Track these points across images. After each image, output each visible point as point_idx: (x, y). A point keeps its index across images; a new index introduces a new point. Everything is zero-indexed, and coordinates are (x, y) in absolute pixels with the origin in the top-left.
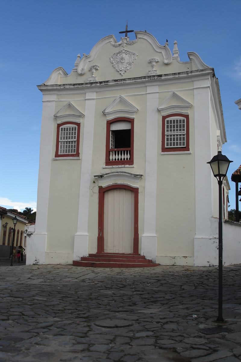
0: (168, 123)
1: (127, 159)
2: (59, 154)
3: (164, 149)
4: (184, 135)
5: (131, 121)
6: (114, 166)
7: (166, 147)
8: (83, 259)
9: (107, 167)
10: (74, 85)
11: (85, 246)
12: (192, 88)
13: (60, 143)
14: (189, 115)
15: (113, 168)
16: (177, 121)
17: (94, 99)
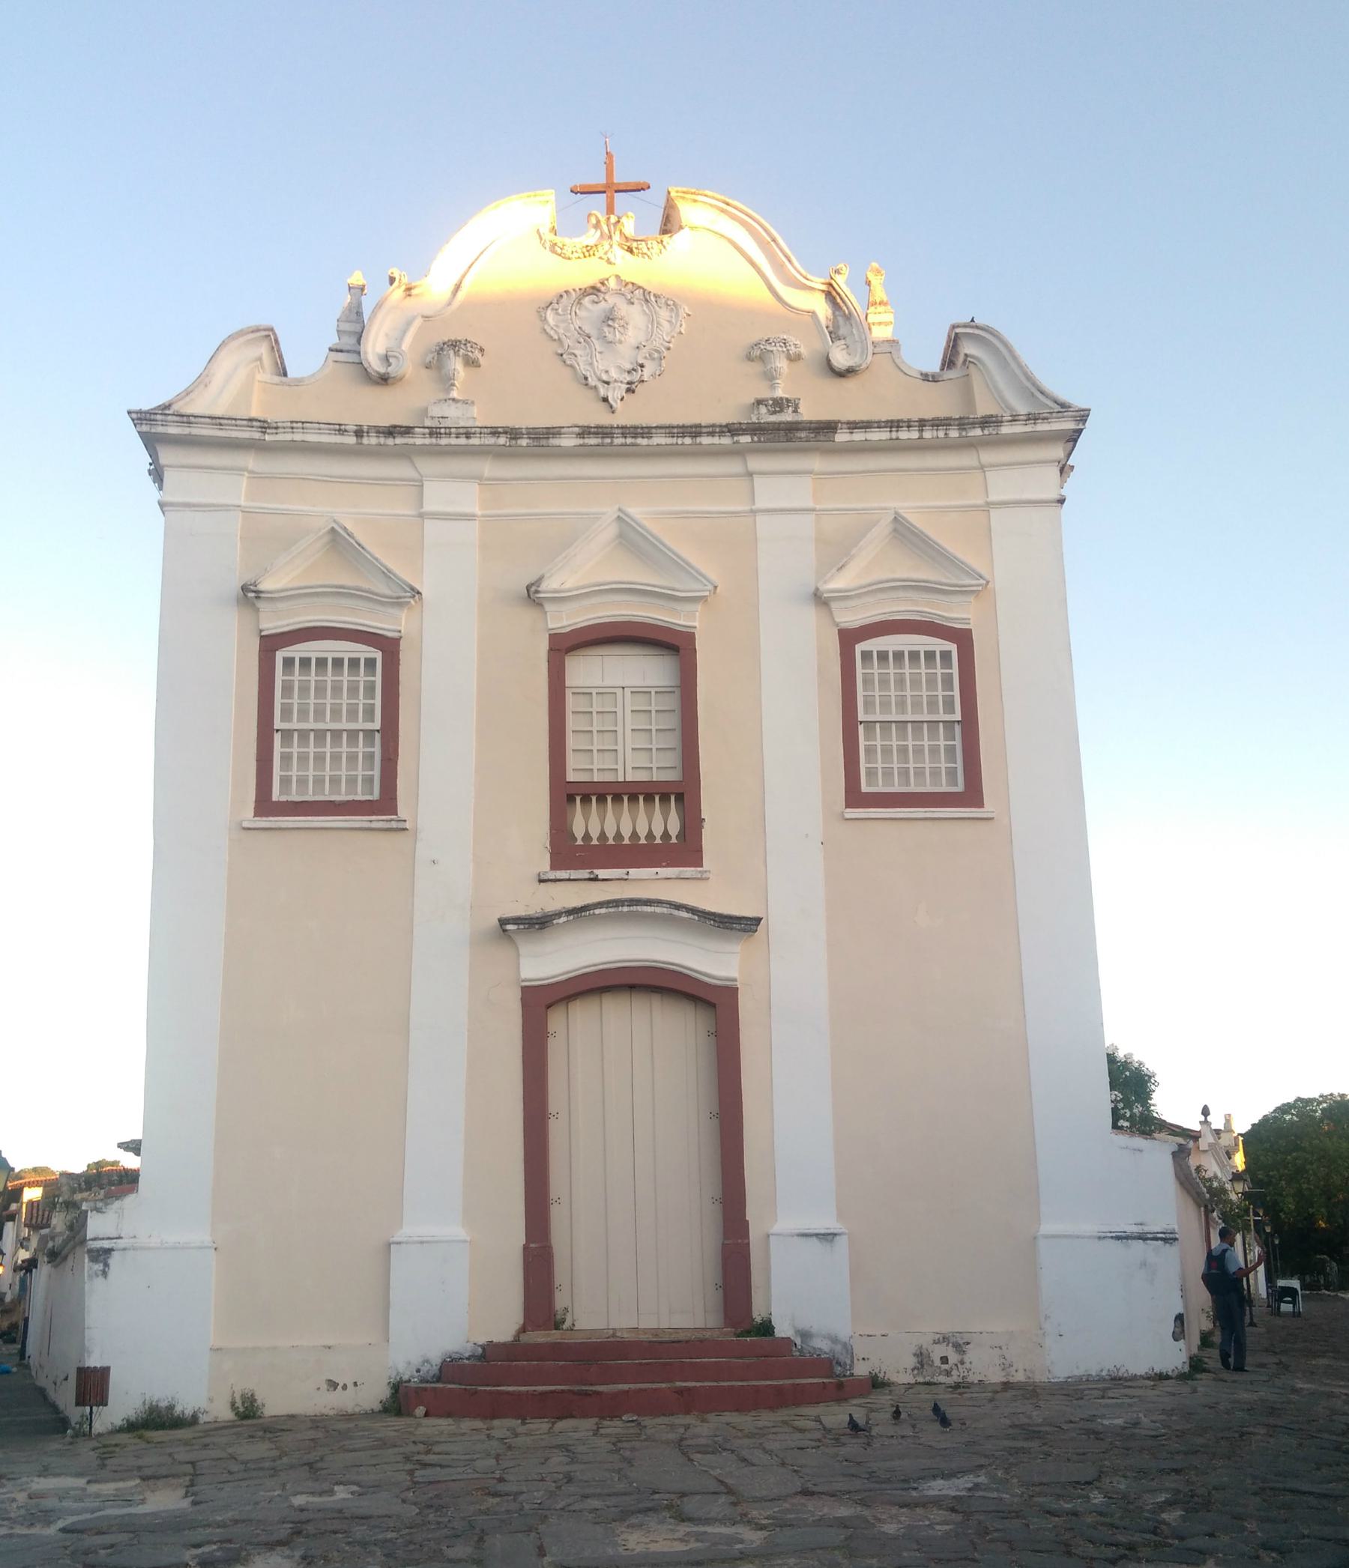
1: (666, 835)
2: (276, 796)
6: (602, 873)
8: (451, 1368)
11: (451, 1300)
12: (980, 502)
13: (277, 738)
14: (970, 630)
15: (596, 879)
17: (469, 517)
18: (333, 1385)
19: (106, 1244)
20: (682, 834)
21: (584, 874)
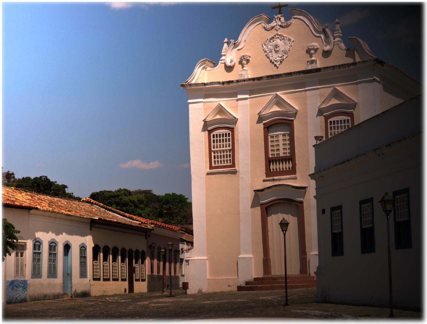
0: (331, 124)
2: (213, 165)
6: (275, 178)
8: (247, 283)
10: (223, 83)
13: (213, 153)
16: (341, 121)
18: (229, 286)
19: (188, 259)
20: (292, 168)
21: (272, 178)
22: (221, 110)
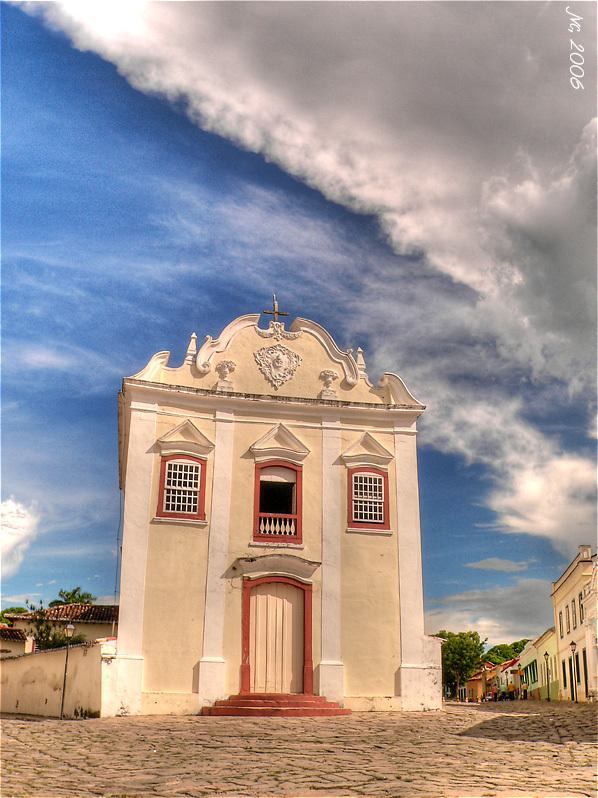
3: (351, 523)
4: (380, 503)
5: (296, 470)
7: (164, 511)
9: (257, 543)
10: (197, 391)
20: (295, 534)
22: (187, 429)
